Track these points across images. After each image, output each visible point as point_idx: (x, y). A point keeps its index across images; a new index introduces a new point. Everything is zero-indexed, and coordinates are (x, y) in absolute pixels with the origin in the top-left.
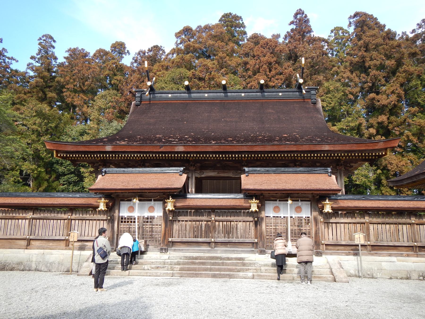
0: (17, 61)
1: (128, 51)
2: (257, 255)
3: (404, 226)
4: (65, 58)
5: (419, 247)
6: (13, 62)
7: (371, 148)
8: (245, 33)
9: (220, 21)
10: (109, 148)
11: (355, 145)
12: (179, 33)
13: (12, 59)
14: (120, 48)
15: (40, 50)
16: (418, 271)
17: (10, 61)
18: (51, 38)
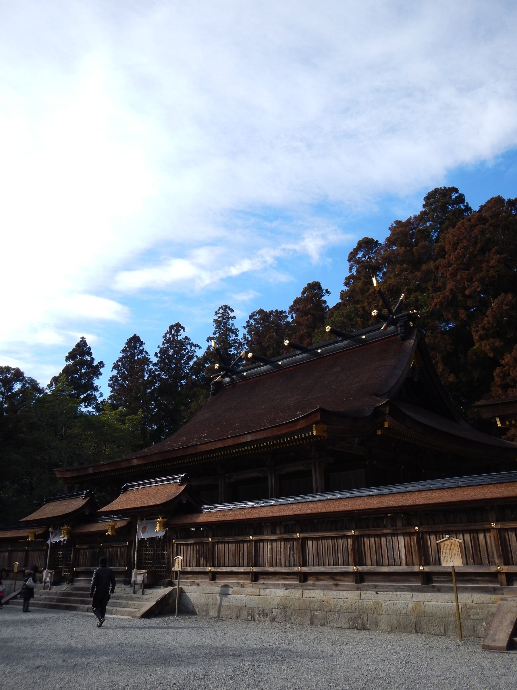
0: (200, 348)
1: (327, 290)
2: (123, 585)
3: (245, 545)
4: (245, 327)
5: (256, 573)
6: (197, 348)
7: (293, 429)
8: (468, 209)
9: (424, 206)
10: (91, 471)
11: (275, 428)
12: (351, 253)
13: (195, 345)
14: (314, 290)
15: (218, 327)
16: (249, 608)
17: (193, 348)
18: (229, 308)
